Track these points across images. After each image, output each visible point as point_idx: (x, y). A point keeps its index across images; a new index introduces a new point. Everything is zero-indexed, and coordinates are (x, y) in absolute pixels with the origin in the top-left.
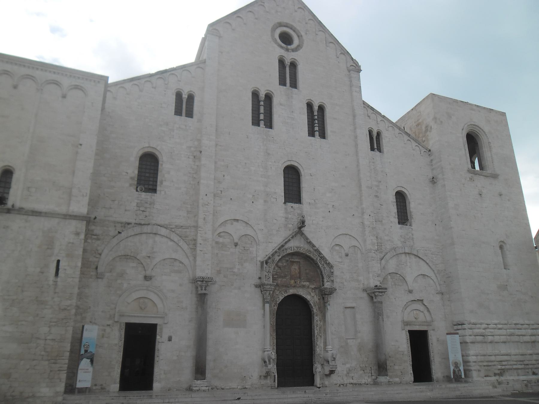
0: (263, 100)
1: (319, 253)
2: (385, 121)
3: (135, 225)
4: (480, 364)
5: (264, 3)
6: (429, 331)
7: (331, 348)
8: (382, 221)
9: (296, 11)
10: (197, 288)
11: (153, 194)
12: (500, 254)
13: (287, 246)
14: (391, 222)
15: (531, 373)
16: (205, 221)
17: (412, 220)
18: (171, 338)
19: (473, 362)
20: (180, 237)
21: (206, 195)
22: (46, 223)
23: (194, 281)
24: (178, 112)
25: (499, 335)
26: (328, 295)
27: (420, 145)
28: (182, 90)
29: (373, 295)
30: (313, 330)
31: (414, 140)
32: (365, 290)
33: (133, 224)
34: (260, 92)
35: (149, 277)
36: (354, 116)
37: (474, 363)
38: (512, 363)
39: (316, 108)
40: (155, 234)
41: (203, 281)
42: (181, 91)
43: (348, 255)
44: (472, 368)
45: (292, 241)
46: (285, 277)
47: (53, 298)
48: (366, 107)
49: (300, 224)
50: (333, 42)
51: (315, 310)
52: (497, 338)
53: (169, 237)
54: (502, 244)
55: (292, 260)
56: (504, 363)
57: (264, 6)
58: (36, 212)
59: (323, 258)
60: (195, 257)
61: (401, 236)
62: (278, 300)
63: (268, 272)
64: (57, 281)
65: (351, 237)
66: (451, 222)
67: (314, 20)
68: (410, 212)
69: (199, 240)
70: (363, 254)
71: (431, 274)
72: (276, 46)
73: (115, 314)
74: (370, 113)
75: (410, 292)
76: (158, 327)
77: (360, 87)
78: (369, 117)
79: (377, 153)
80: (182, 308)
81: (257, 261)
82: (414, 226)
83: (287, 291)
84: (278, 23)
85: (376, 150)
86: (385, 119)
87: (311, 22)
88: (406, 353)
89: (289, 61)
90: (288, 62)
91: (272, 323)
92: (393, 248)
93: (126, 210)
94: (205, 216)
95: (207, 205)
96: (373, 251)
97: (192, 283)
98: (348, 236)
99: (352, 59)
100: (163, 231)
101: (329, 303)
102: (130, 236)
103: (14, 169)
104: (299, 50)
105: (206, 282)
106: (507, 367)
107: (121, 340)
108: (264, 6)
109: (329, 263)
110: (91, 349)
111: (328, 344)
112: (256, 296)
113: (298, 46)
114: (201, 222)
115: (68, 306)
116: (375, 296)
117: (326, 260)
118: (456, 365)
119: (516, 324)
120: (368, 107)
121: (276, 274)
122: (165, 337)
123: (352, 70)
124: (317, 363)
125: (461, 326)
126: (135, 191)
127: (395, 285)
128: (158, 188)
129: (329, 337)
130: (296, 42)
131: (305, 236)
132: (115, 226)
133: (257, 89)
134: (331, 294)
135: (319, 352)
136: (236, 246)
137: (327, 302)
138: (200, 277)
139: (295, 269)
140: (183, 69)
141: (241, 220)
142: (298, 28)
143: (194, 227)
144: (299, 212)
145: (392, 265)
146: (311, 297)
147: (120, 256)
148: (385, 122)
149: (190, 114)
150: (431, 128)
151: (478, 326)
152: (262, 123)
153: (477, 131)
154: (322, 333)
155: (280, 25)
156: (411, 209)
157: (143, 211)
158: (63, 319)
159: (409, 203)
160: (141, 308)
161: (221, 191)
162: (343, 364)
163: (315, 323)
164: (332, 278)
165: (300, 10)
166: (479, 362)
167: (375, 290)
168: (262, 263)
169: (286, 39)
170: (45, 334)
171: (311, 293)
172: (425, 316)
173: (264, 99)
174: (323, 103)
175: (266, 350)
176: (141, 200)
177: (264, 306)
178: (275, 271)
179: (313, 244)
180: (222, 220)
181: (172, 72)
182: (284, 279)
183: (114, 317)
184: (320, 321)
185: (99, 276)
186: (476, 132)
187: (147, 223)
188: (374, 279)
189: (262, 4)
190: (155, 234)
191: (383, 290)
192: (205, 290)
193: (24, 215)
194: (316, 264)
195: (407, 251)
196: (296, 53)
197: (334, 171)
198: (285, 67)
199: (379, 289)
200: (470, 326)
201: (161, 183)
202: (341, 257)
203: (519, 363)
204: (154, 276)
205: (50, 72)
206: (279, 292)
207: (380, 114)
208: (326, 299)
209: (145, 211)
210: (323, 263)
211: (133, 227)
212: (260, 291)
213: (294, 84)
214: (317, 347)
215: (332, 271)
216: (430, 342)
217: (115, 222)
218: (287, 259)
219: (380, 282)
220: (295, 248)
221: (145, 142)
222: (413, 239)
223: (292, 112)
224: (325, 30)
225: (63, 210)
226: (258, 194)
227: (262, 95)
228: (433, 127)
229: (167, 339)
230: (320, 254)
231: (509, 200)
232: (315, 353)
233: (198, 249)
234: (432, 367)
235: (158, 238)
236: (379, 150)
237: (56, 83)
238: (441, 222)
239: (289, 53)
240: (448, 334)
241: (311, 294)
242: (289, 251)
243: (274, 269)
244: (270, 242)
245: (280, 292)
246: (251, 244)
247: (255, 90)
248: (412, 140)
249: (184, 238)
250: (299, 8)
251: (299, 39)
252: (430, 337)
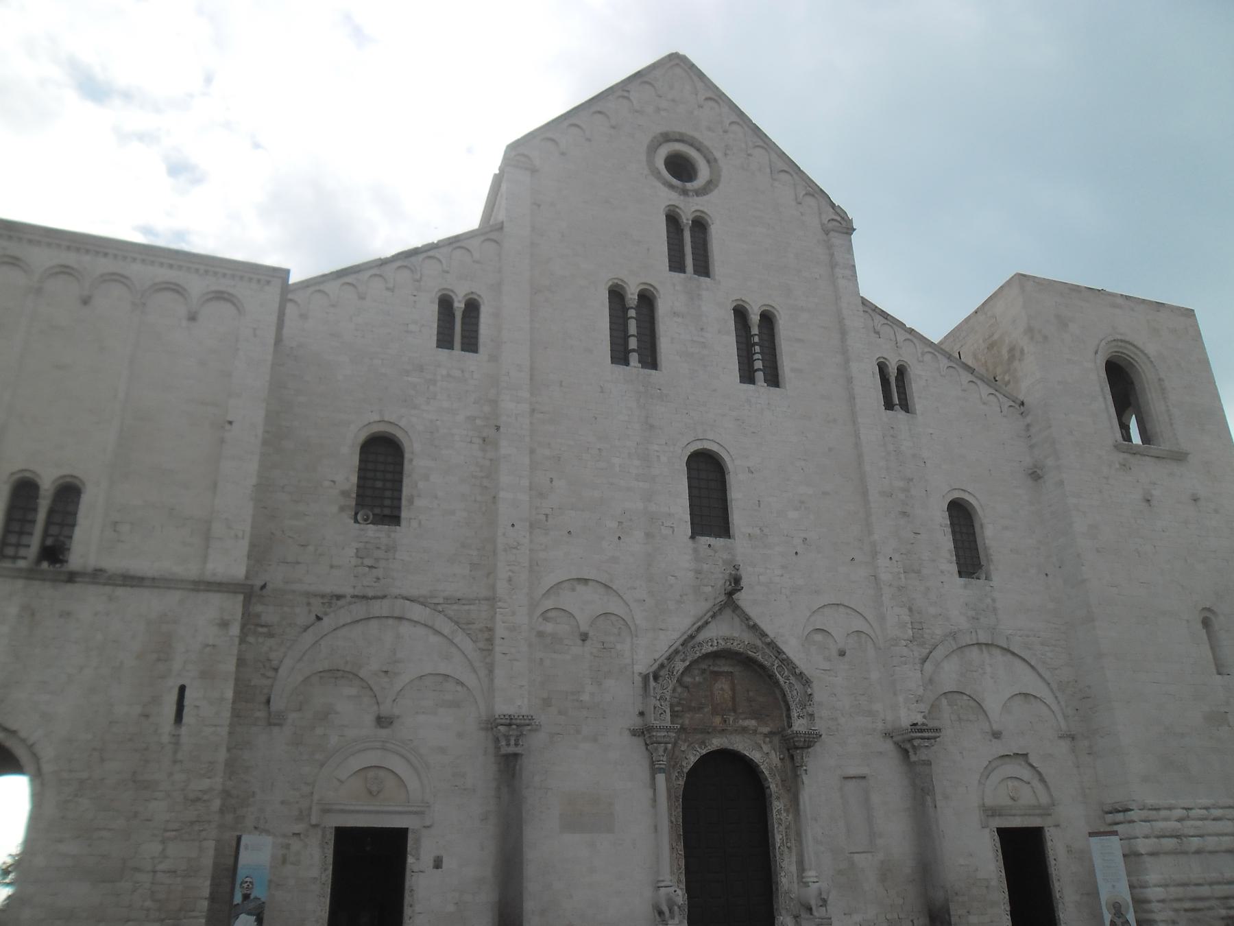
0: (634, 306)
1: (778, 652)
2: (915, 340)
3: (353, 600)
4: (1176, 905)
5: (628, 91)
6: (1046, 829)
7: (816, 877)
8: (919, 572)
9: (701, 106)
10: (497, 740)
11: (393, 528)
12: (1205, 637)
13: (701, 637)
14: (942, 572)
16: (511, 585)
17: (992, 567)
18: (442, 861)
19: (1159, 901)
20: (457, 623)
21: (513, 525)
22: (151, 603)
23: (490, 726)
24: (445, 341)
25: (1218, 835)
26: (802, 748)
27: (1000, 393)
28: (452, 291)
29: (908, 746)
30: (770, 834)
31: (984, 381)
32: (888, 735)
33: (349, 596)
34: (627, 288)
35: (386, 718)
36: (843, 333)
37: (1160, 905)
39: (755, 318)
40: (400, 618)
41: (510, 725)
42: (451, 294)
43: (845, 653)
44: (1157, 917)
45: (712, 626)
46: (700, 709)
48: (870, 311)
49: (730, 585)
50: (785, 169)
51: (773, 787)
52: (1211, 842)
53: (430, 624)
54: (1207, 614)
55: (716, 669)
57: (628, 98)
58: (133, 578)
59: (786, 662)
60: (491, 671)
61: (966, 604)
62: (685, 765)
63: (659, 700)
64: (179, 735)
65: (849, 611)
66: (1083, 568)
67: (741, 122)
68: (986, 548)
69: (500, 631)
70: (880, 649)
71: (1042, 691)
72: (659, 185)
73: (310, 808)
74: (879, 326)
75: (997, 735)
76: (411, 836)
77: (854, 266)
78: (878, 333)
79: (900, 415)
80: (465, 789)
81: (633, 673)
82: (996, 580)
83: (707, 741)
84: (662, 134)
85: (898, 407)
86: (915, 337)
87: (734, 127)
88: (994, 883)
89: (691, 218)
90: (687, 220)
91: (673, 819)
92: (951, 633)
93: (332, 567)
94: (510, 574)
95: (516, 548)
96: (904, 643)
97: (486, 729)
98: (842, 609)
99: (833, 205)
100: (417, 612)
101: (805, 768)
102: (344, 625)
103: (84, 484)
104: (711, 191)
105: (517, 726)
107: (325, 870)
108: (628, 98)
109: (801, 673)
110: (258, 892)
111: (807, 866)
112: (634, 757)
113: (710, 182)
114: (502, 588)
115: (204, 792)
116: (914, 747)
117: (795, 667)
118: (1117, 909)
120: (874, 310)
121: (679, 704)
122: (427, 859)
123: (833, 230)
124: (783, 912)
125: (1122, 814)
126: (353, 521)
127: (960, 720)
129: (810, 848)
130: (704, 173)
131: (743, 612)
132: (309, 604)
133: (620, 283)
134: (809, 747)
135: (786, 887)
136: (583, 640)
137: (802, 766)
138: (504, 716)
139: (722, 689)
140: (455, 245)
141: (594, 580)
142: (707, 143)
143: (487, 599)
145: (949, 674)
146: (764, 756)
147: (321, 672)
148: (914, 344)
149: (471, 345)
150: (1022, 351)
151: (1163, 813)
152: (634, 358)
153: (1130, 354)
154: (793, 840)
155: (667, 138)
156: (987, 541)
157: (371, 567)
158: (192, 823)
159: (982, 526)
160: (370, 793)
161: (547, 515)
162: (845, 914)
163: (775, 816)
164: (810, 710)
165: (711, 103)
166: (1172, 900)
167: (912, 734)
168: (645, 678)
169: (680, 168)
170: (153, 858)
171: (763, 746)
172: (1034, 792)
173: (636, 303)
174: (770, 306)
175: (662, 884)
176: (367, 542)
177: (653, 779)
178: (677, 695)
179: (763, 631)
180: (549, 580)
181: (430, 253)
182: (697, 715)
183: (309, 815)
184: (787, 811)
185: (274, 721)
186: (1128, 355)
187: (379, 594)
188: (909, 709)
189: (626, 94)
190: (400, 618)
191: (930, 734)
192: (516, 745)
193: (105, 584)
194: (771, 676)
195: (982, 640)
196: (706, 198)
197: (804, 460)
198: (682, 230)
199: (921, 731)
200: (1145, 814)
201: (411, 501)
204: (398, 717)
205: (162, 265)
206: (686, 744)
207: (902, 325)
208: (798, 758)
209: (376, 568)
210: (786, 673)
211: (350, 603)
212: (643, 744)
213: (703, 268)
214: (783, 874)
215: (809, 691)
216: (1051, 854)
217: (308, 594)
218: (704, 666)
219: (923, 714)
220: (720, 641)
221: (372, 412)
222: (995, 610)
223: (702, 329)
224: (767, 145)
225: (191, 570)
226: (631, 520)
227: (632, 296)
228: (1026, 351)
229: (431, 864)
230: (779, 653)
231: (1216, 511)
232: (777, 889)
233: (498, 649)
234: (1059, 916)
235: (405, 628)
236: (905, 406)
237: (176, 289)
238: (1060, 567)
239: (690, 199)
240: (1091, 834)
241: (762, 748)
242: (707, 649)
243: (674, 690)
244: (661, 629)
245: (688, 746)
246: (619, 634)
247: (617, 285)
248: (979, 382)
249: (464, 626)
250: (707, 99)
251: (710, 167)
252: (1049, 844)
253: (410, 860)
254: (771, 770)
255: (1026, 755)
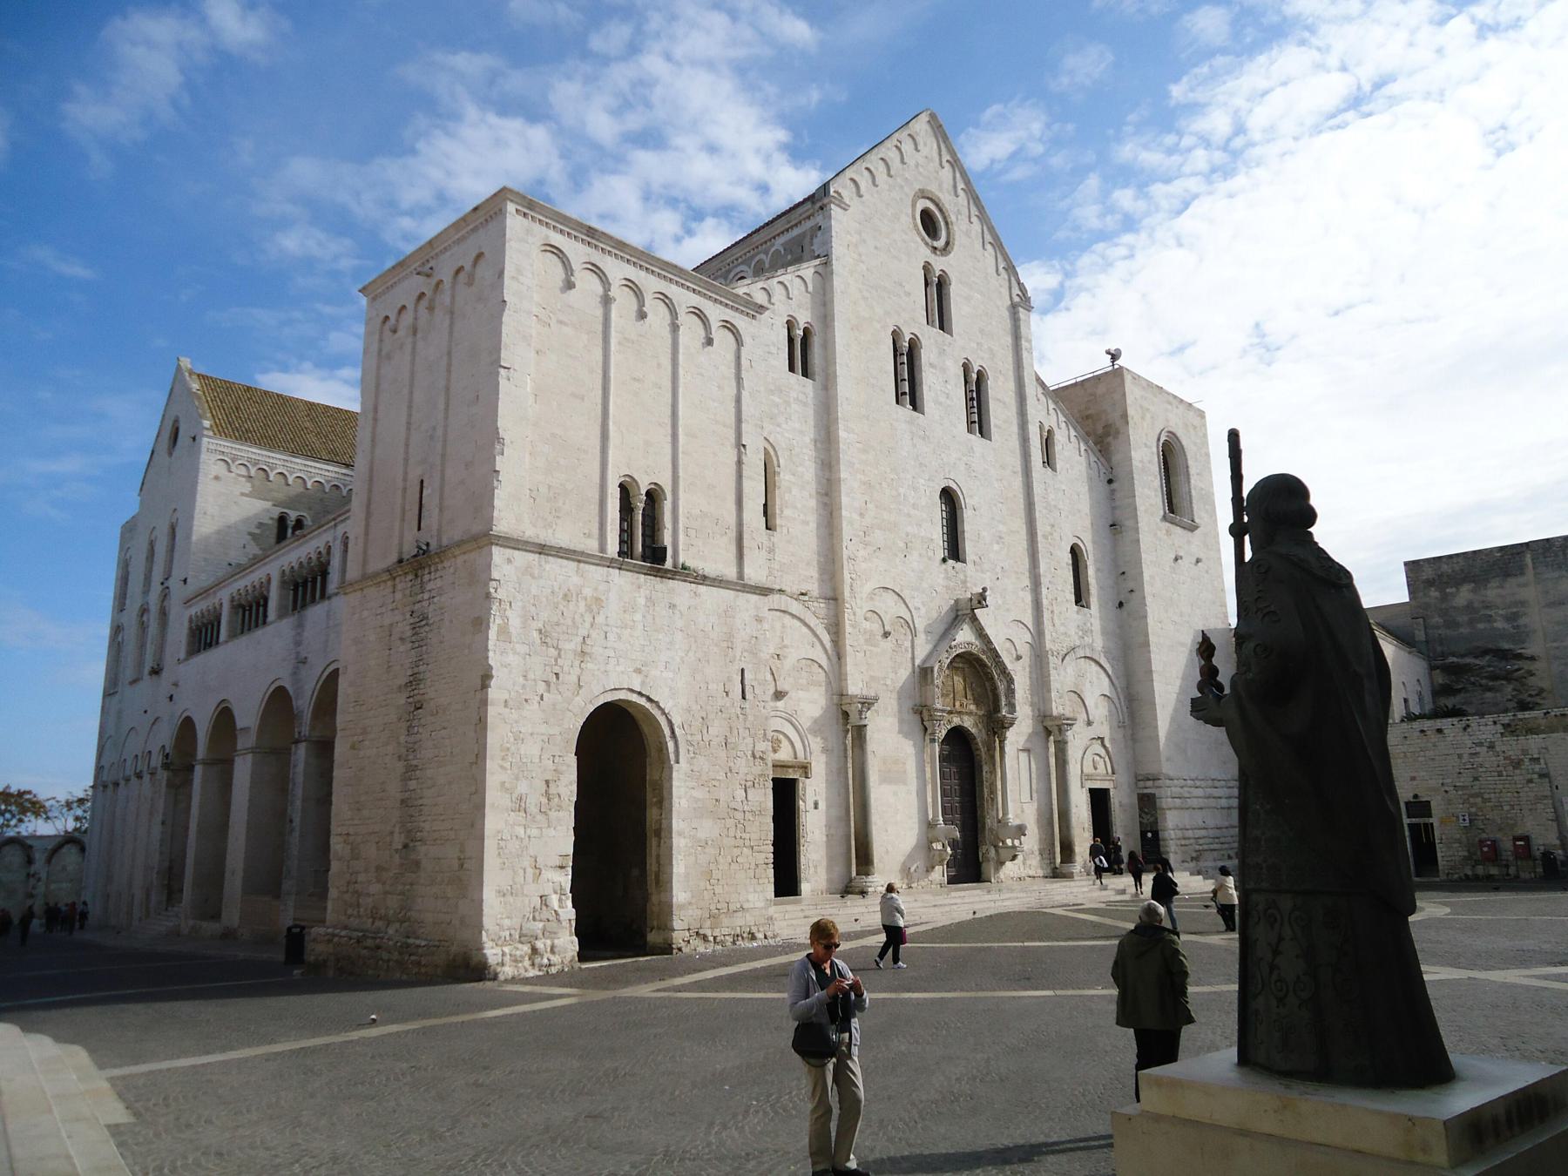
4: (1179, 842)
15: (1226, 857)
24: (792, 369)
38: (1208, 841)
40: (784, 612)
47: (744, 738)
56: (1201, 841)
69: (848, 629)
72: (919, 240)
76: (801, 785)
88: (1086, 826)
106: (1206, 847)
113: (947, 243)
117: (1005, 668)
119: (1213, 780)
125: (1151, 782)
128: (778, 522)
142: (947, 206)
144: (962, 577)
150: (1118, 432)
155: (923, 194)
169: (928, 223)
199: (1068, 719)
202: (1011, 662)
203: (1217, 840)
213: (944, 325)
225: (730, 573)
229: (813, 806)
231: (1207, 572)
235: (787, 619)
239: (937, 258)
250: (948, 161)
251: (948, 228)
253: (801, 802)
254: (982, 742)
255: (1102, 739)
